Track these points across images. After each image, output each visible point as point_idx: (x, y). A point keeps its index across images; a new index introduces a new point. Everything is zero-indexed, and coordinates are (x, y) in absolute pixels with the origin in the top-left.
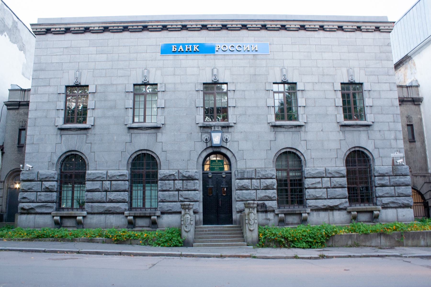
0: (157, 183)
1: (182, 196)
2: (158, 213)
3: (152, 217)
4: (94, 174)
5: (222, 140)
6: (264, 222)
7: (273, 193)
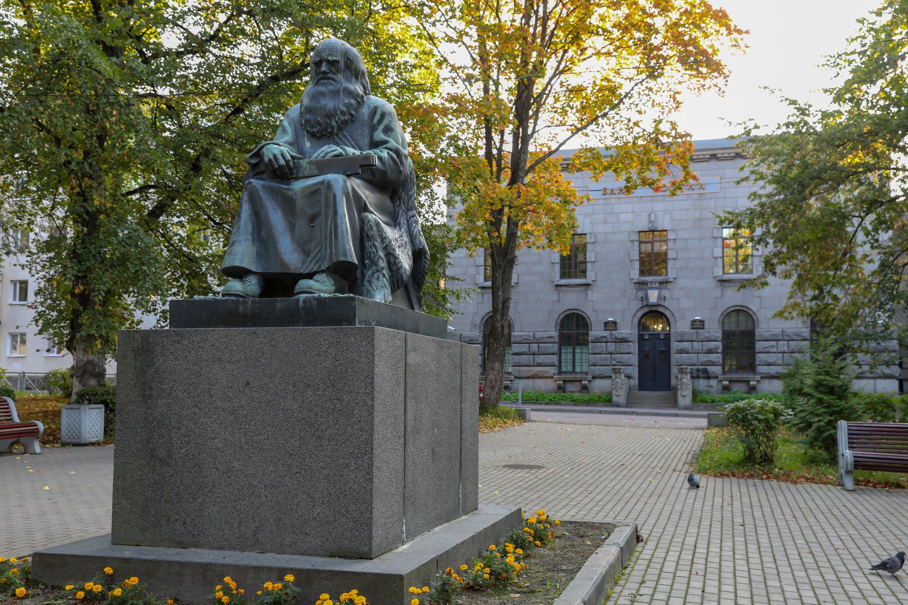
0: (588, 345)
1: (614, 359)
2: (590, 377)
3: (583, 382)
4: (520, 336)
5: (659, 297)
6: (706, 389)
7: (717, 357)
